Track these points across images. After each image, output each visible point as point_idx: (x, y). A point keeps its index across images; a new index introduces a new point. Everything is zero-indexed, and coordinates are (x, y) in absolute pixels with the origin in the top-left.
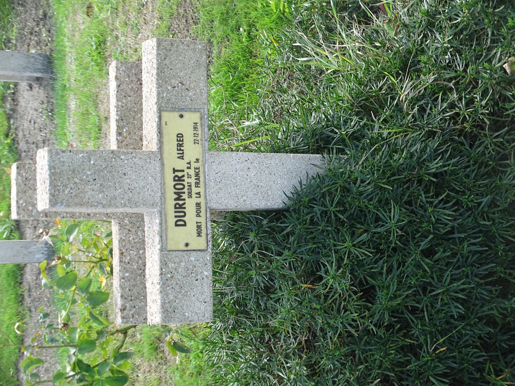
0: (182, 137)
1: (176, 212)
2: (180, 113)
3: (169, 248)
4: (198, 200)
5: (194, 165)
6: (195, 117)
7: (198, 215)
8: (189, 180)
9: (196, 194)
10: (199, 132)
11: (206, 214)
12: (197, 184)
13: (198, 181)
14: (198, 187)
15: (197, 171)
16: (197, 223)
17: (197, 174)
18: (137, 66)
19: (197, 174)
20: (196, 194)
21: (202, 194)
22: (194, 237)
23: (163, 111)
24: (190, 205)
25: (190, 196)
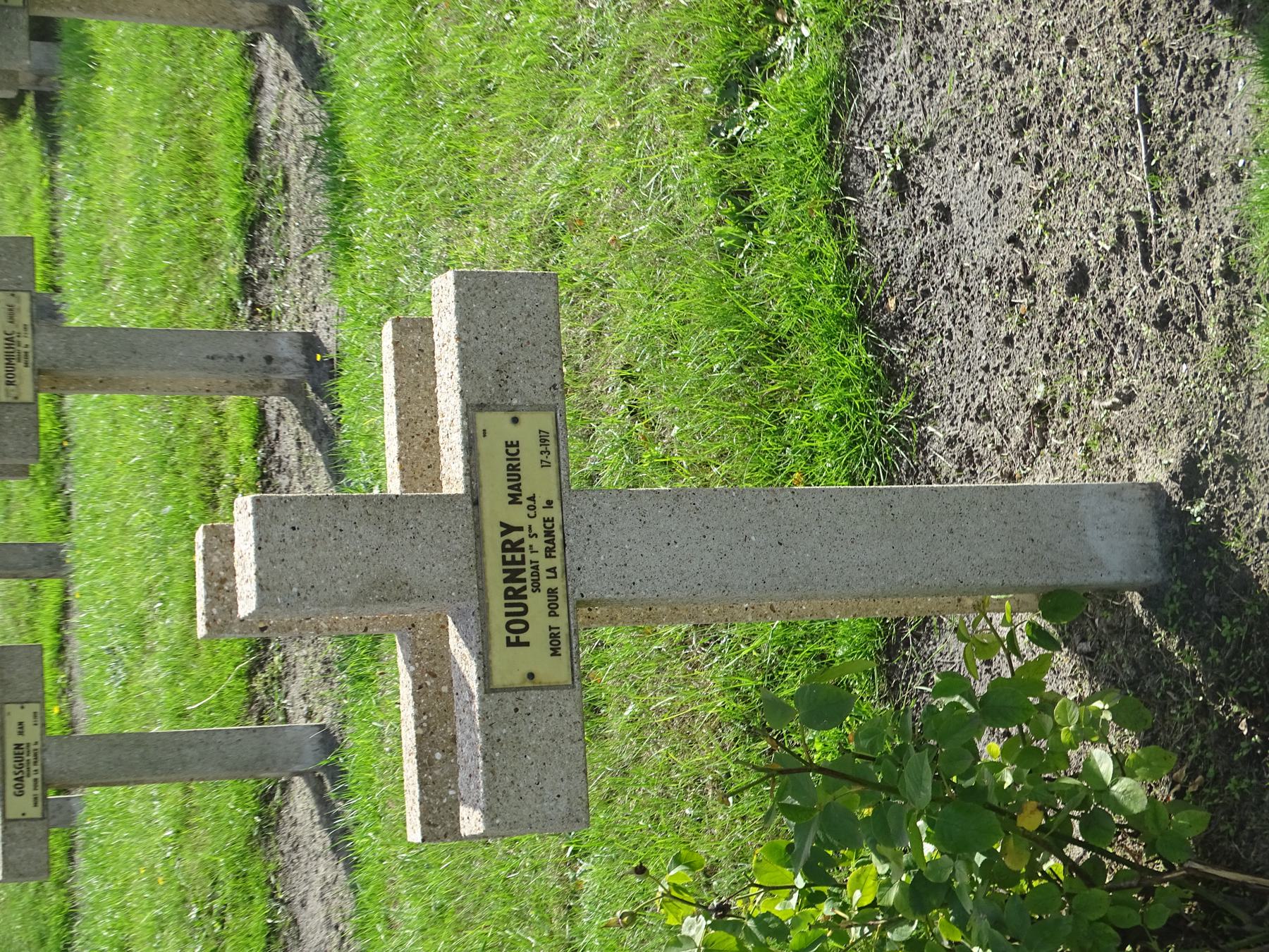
1: (507, 605)
3: (498, 681)
4: (553, 584)
6: (545, 421)
7: (552, 613)
9: (548, 570)
10: (552, 448)
12: (549, 553)
14: (551, 557)
16: (550, 628)
17: (549, 533)
18: (425, 326)
19: (549, 533)
20: (548, 570)
21: (559, 571)
23: (481, 407)
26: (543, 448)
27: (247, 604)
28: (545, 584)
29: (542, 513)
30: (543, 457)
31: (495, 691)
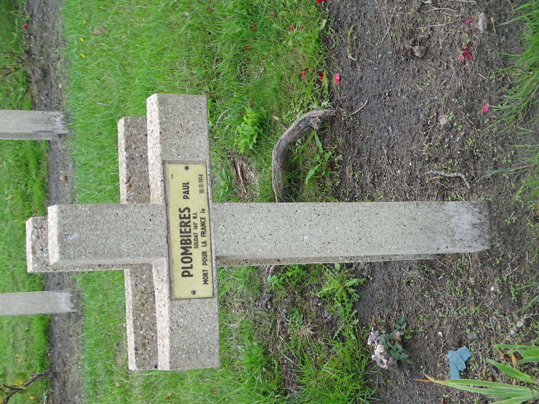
4: (205, 249)
5: (200, 215)
7: (204, 264)
9: (203, 243)
10: (205, 183)
11: (212, 263)
12: (203, 234)
13: (204, 231)
14: (204, 236)
15: (203, 221)
16: (203, 271)
17: (203, 224)
20: (203, 243)
21: (208, 243)
25: (196, 246)
26: (200, 184)
27: (54, 256)
28: (202, 249)
29: (200, 215)
30: (201, 188)
31: (176, 299)
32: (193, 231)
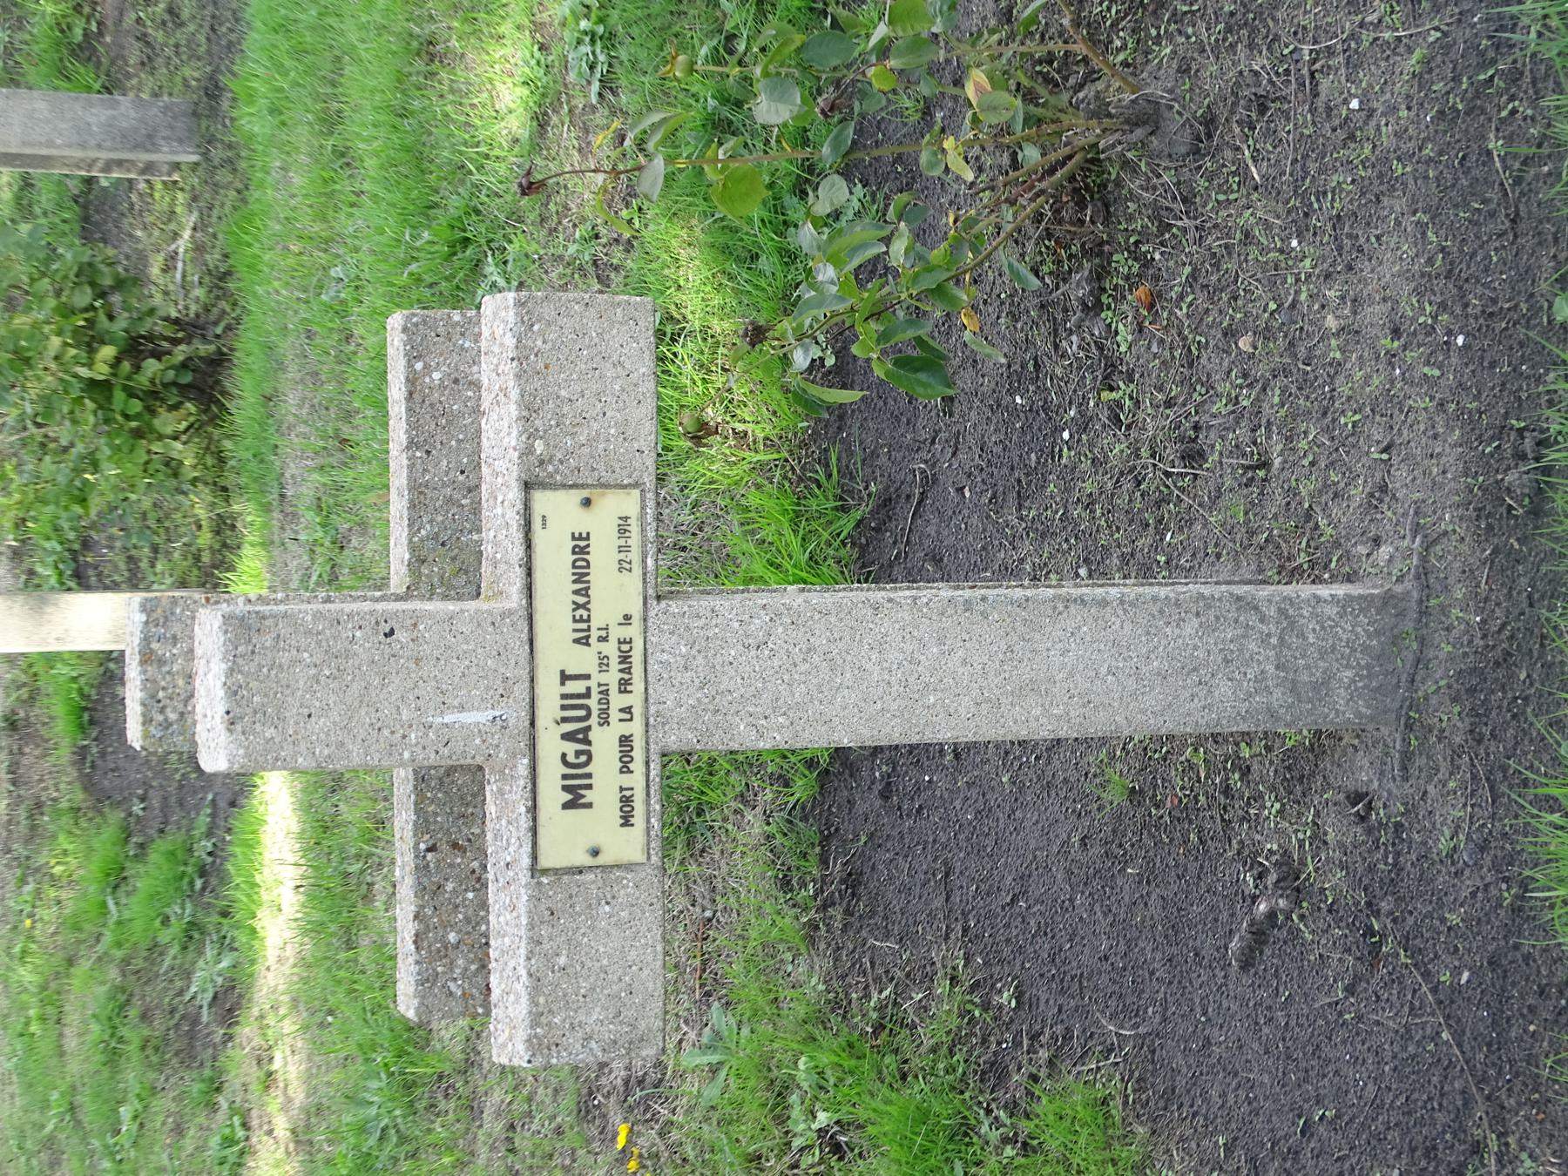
0: (588, 566)
2: (585, 493)
4: (626, 729)
5: (617, 633)
6: (628, 504)
7: (625, 769)
8: (603, 678)
13: (627, 677)
14: (626, 691)
15: (625, 647)
16: (622, 789)
17: (625, 658)
19: (625, 658)
22: (609, 831)
24: (604, 742)
25: (605, 721)
28: (617, 729)
29: (617, 633)
32: (597, 678)
